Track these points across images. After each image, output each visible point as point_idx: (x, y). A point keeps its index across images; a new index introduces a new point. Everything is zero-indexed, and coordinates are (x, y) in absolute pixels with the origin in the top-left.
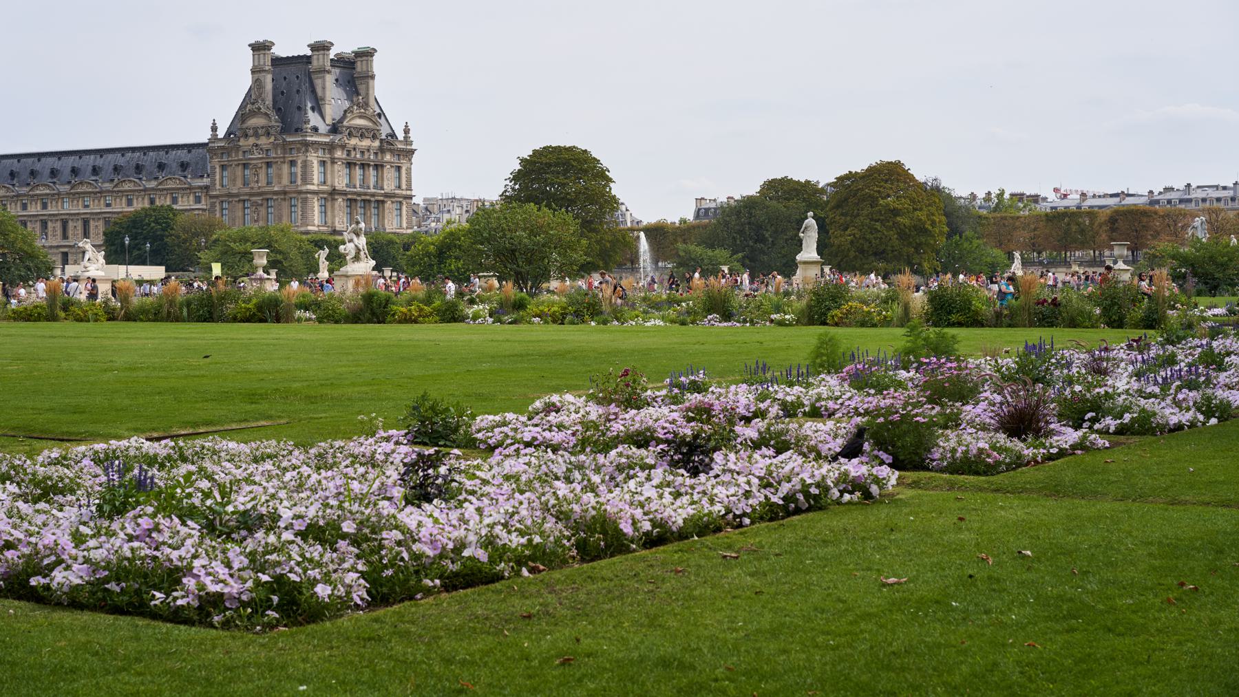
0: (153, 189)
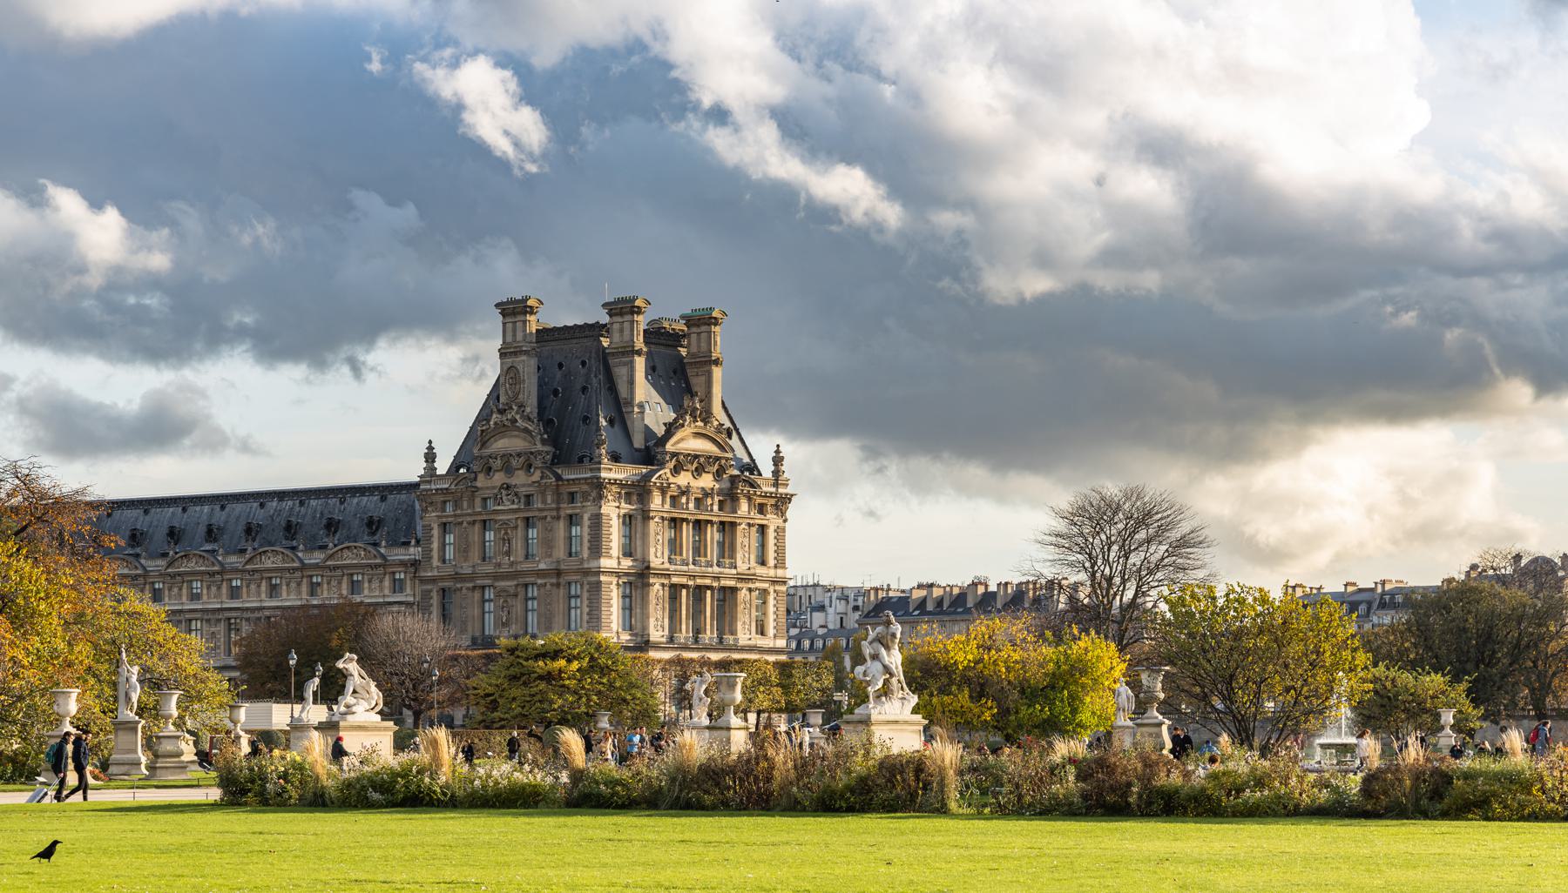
0: (316, 566)
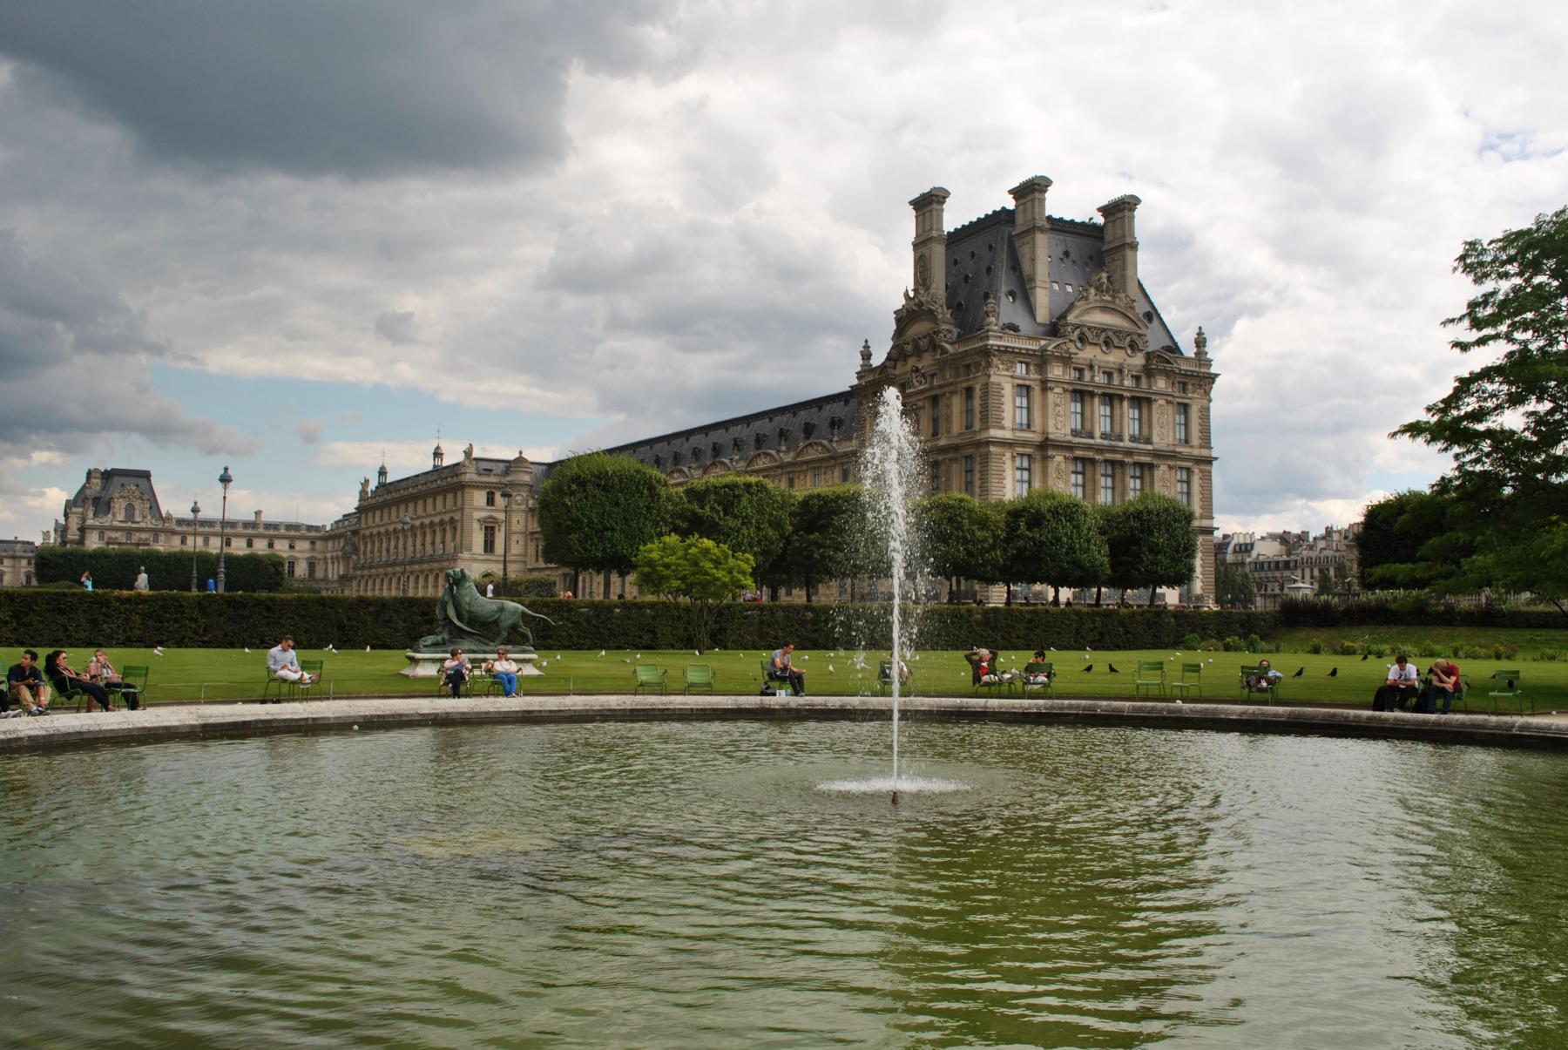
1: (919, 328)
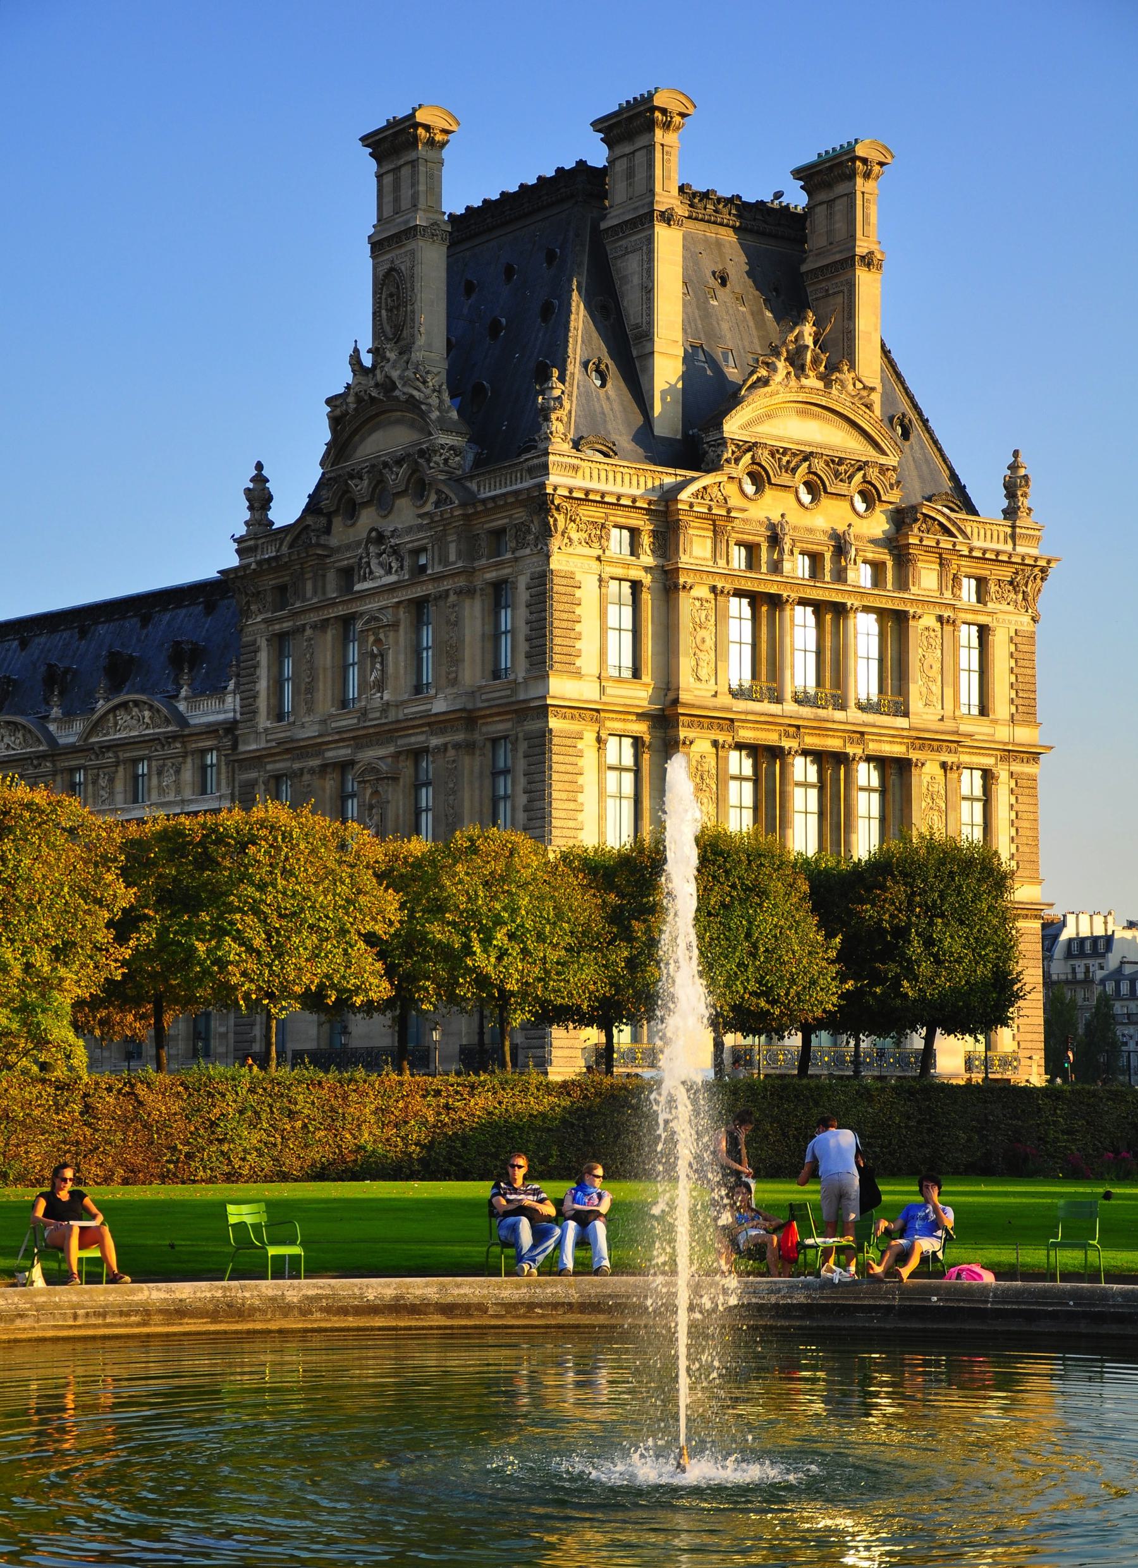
0: (73, 750)
1: (388, 441)
